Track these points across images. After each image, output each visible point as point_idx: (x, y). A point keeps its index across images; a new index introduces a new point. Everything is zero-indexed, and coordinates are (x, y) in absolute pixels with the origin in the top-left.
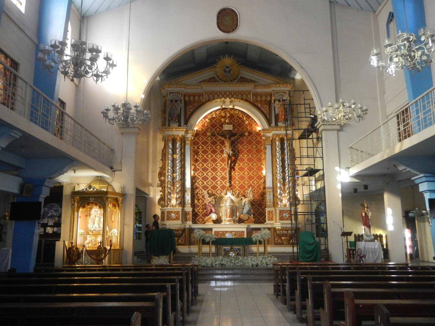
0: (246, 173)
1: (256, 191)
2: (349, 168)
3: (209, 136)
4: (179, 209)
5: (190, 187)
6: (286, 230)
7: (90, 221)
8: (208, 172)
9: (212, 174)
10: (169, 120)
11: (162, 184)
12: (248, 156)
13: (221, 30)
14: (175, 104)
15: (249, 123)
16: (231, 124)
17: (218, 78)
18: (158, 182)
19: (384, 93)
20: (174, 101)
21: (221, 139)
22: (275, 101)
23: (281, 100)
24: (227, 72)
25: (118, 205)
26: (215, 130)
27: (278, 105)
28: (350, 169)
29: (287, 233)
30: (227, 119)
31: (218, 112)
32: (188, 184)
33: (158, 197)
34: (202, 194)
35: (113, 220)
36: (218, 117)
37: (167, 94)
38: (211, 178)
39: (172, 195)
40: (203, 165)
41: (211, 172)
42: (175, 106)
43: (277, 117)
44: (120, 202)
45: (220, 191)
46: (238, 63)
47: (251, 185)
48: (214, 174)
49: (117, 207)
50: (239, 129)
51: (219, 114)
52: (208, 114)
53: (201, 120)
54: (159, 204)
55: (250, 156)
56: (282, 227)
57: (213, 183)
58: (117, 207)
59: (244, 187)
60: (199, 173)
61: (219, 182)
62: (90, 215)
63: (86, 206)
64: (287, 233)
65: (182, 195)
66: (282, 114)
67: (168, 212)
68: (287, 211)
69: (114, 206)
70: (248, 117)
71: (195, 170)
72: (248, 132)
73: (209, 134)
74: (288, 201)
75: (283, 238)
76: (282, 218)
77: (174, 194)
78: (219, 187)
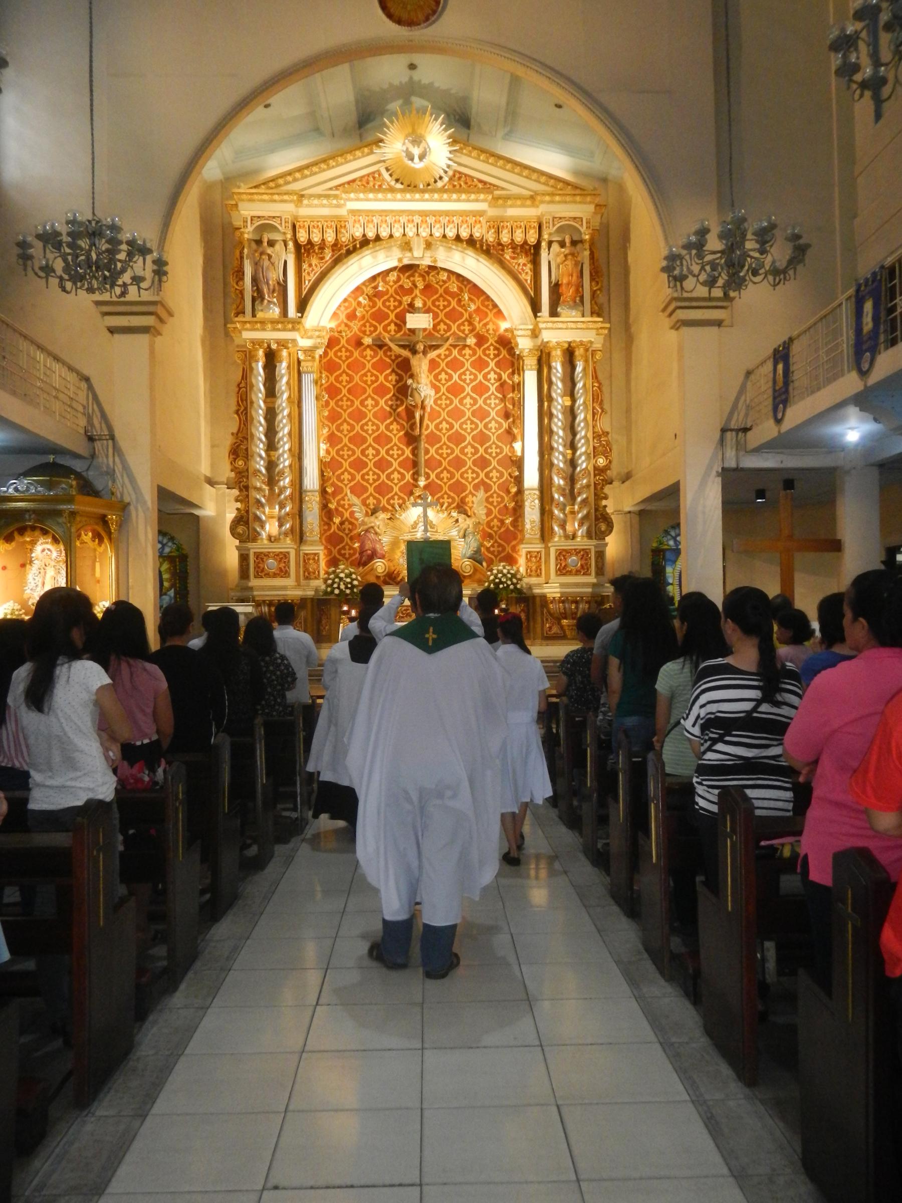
0: (469, 450)
1: (495, 499)
2: (745, 430)
3: (368, 346)
4: (288, 546)
5: (317, 486)
6: (573, 602)
7: (30, 577)
8: (367, 448)
9: (378, 452)
10: (254, 300)
11: (241, 482)
12: (475, 401)
13: (390, 16)
14: (269, 251)
15: (478, 310)
16: (427, 311)
17: (391, 175)
18: (226, 473)
19: (855, 216)
20: (265, 244)
21: (400, 356)
22: (550, 243)
23: (568, 241)
24: (416, 159)
25: (109, 534)
26: (385, 329)
27: (558, 255)
28: (749, 434)
29: (577, 608)
30: (416, 296)
31: (393, 277)
32: (312, 480)
33: (230, 516)
34: (350, 506)
35: (98, 574)
36: (391, 291)
37: (245, 221)
38: (375, 465)
39: (267, 509)
40: (353, 428)
41: (374, 448)
42: (270, 257)
43: (555, 288)
44: (113, 528)
45: (400, 498)
46: (445, 130)
47: (483, 482)
48: (383, 452)
49: (106, 541)
50: (449, 328)
51: (395, 282)
52: (364, 284)
53: (345, 300)
54: (233, 535)
55: (480, 402)
56: (561, 593)
57: (379, 477)
58: (106, 541)
59: (464, 488)
60: (342, 449)
61: (396, 476)
62: (31, 562)
63: (16, 534)
64: (577, 608)
65: (296, 511)
66: (568, 284)
67: (258, 555)
68: (577, 552)
69: (98, 537)
70: (476, 291)
71: (332, 439)
72: (474, 336)
73: (368, 341)
74: (581, 524)
75: (565, 622)
76: (562, 571)
77: (272, 507)
78: (396, 489)
